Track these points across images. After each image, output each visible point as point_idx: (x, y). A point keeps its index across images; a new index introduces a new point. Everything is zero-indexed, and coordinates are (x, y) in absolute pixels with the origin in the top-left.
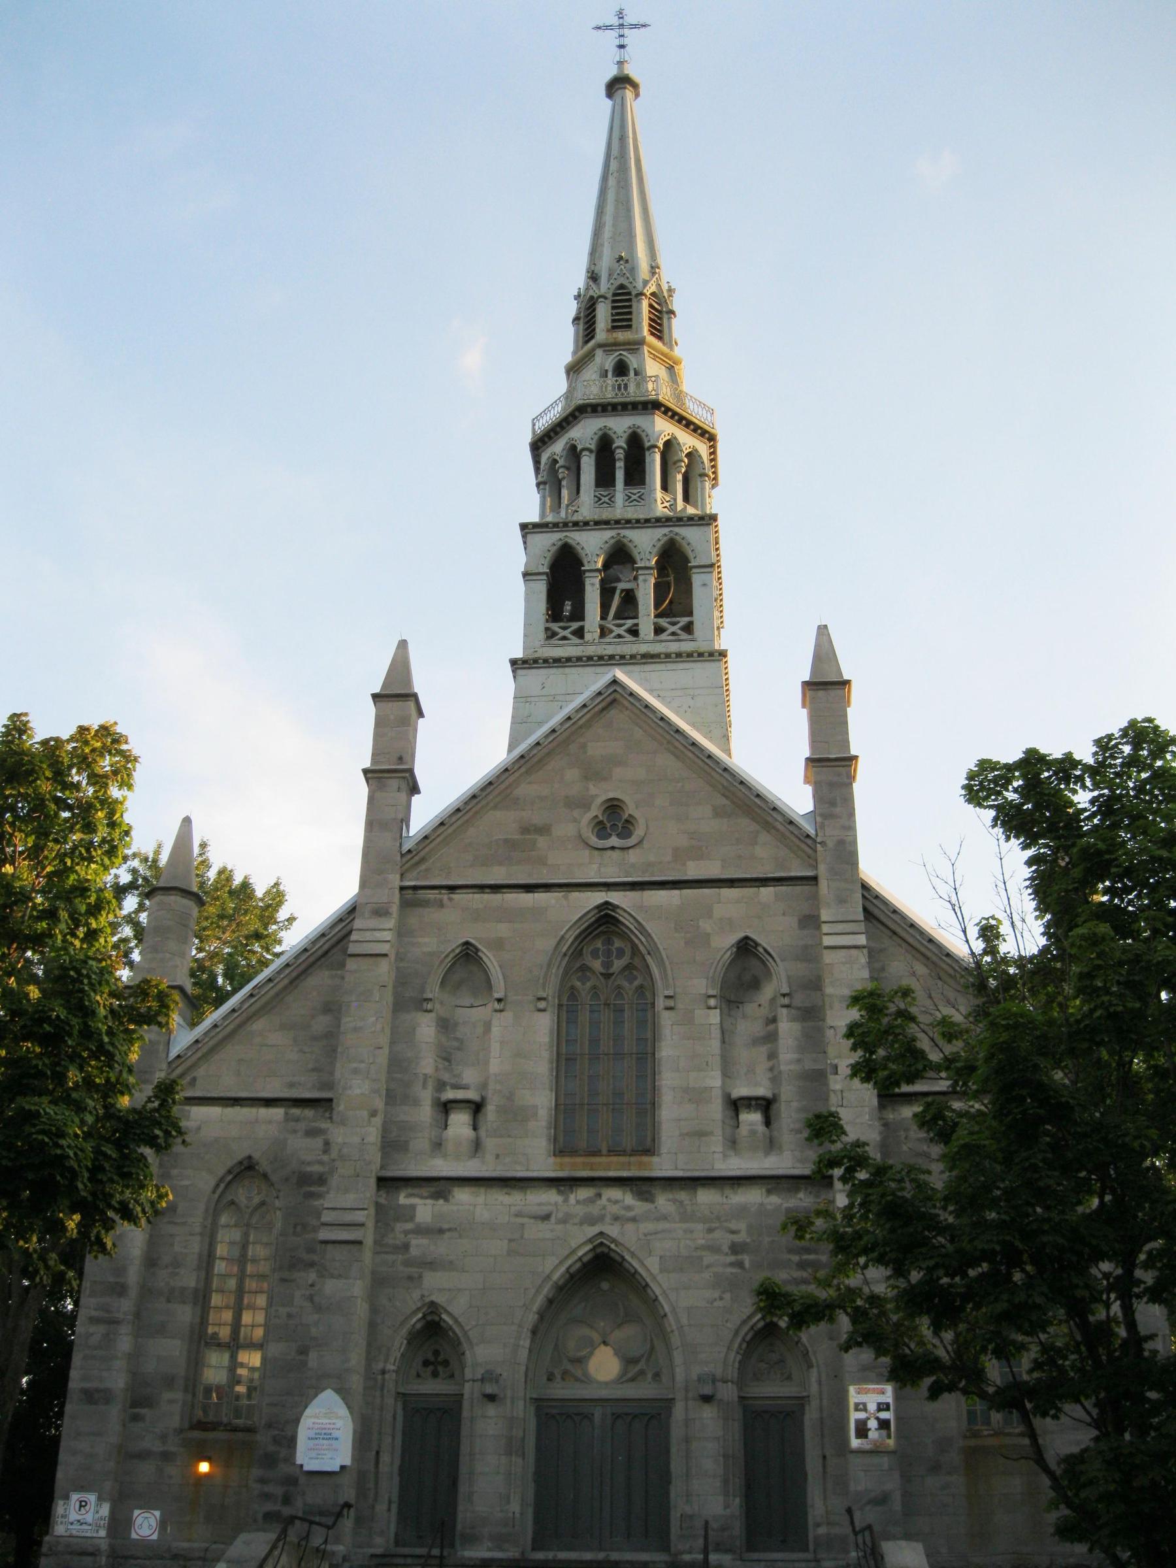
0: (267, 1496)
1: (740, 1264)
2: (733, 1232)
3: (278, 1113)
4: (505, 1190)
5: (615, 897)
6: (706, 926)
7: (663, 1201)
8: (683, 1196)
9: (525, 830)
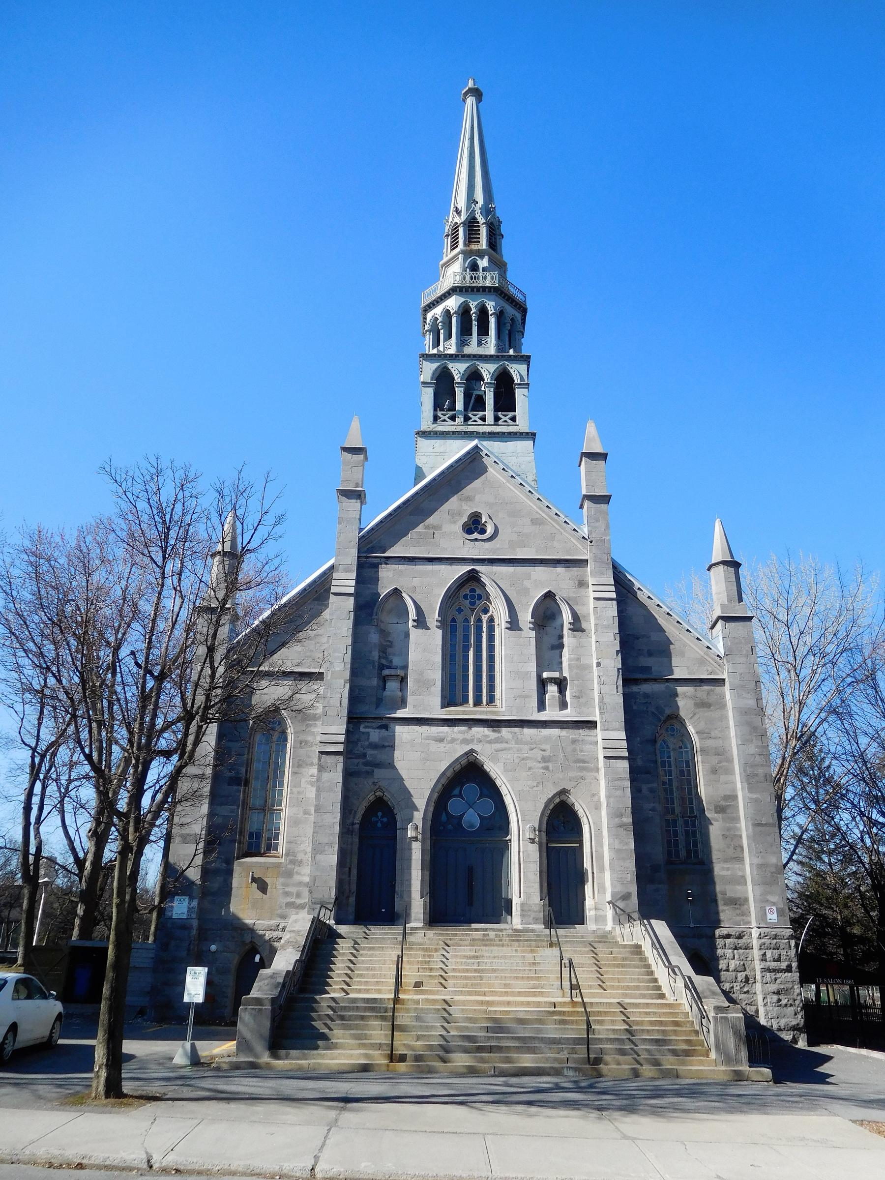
0: (287, 894)
1: (547, 768)
2: (544, 750)
5: (478, 568)
6: (527, 583)
7: (505, 732)
8: (516, 730)
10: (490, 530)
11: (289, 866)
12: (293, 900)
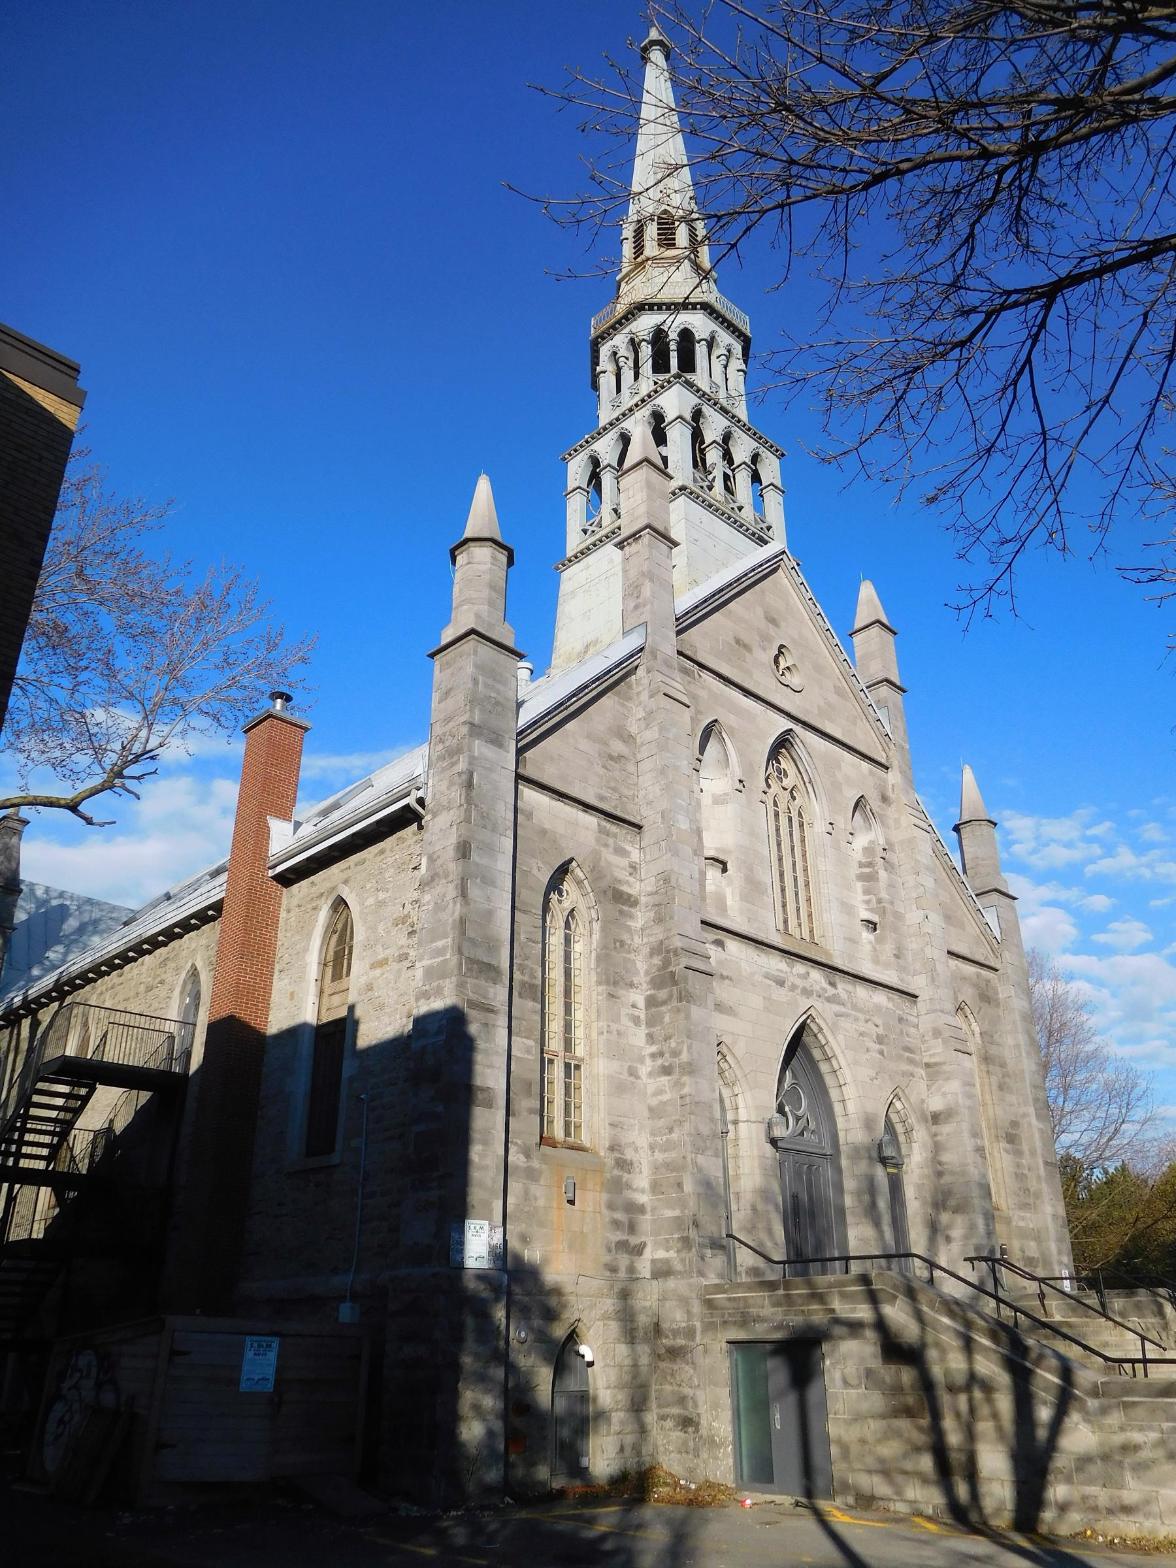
3: (591, 821)
4: (757, 952)
7: (843, 987)
9: (738, 641)
10: (794, 680)
11: (616, 1172)
12: (625, 1238)
